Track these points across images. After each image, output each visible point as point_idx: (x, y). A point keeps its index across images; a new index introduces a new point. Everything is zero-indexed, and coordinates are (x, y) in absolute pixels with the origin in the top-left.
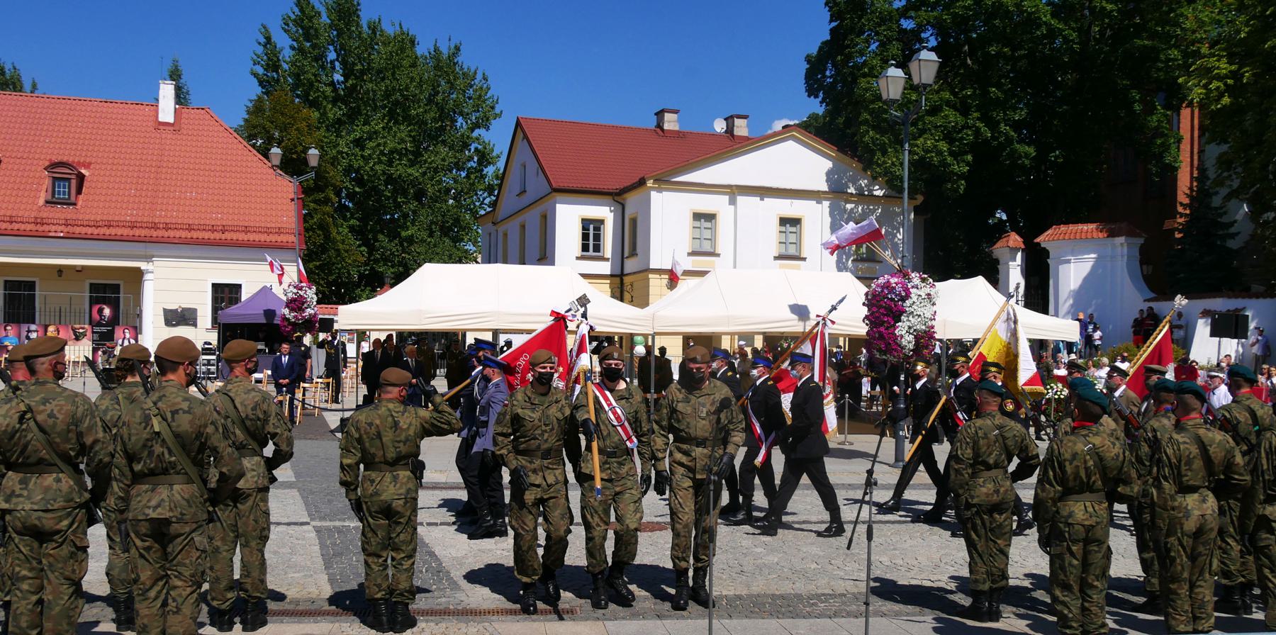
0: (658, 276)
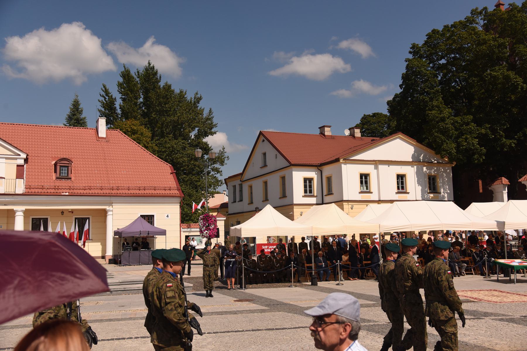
0: (347, 204)
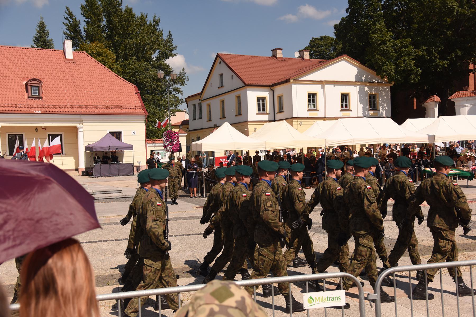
0: (296, 120)
